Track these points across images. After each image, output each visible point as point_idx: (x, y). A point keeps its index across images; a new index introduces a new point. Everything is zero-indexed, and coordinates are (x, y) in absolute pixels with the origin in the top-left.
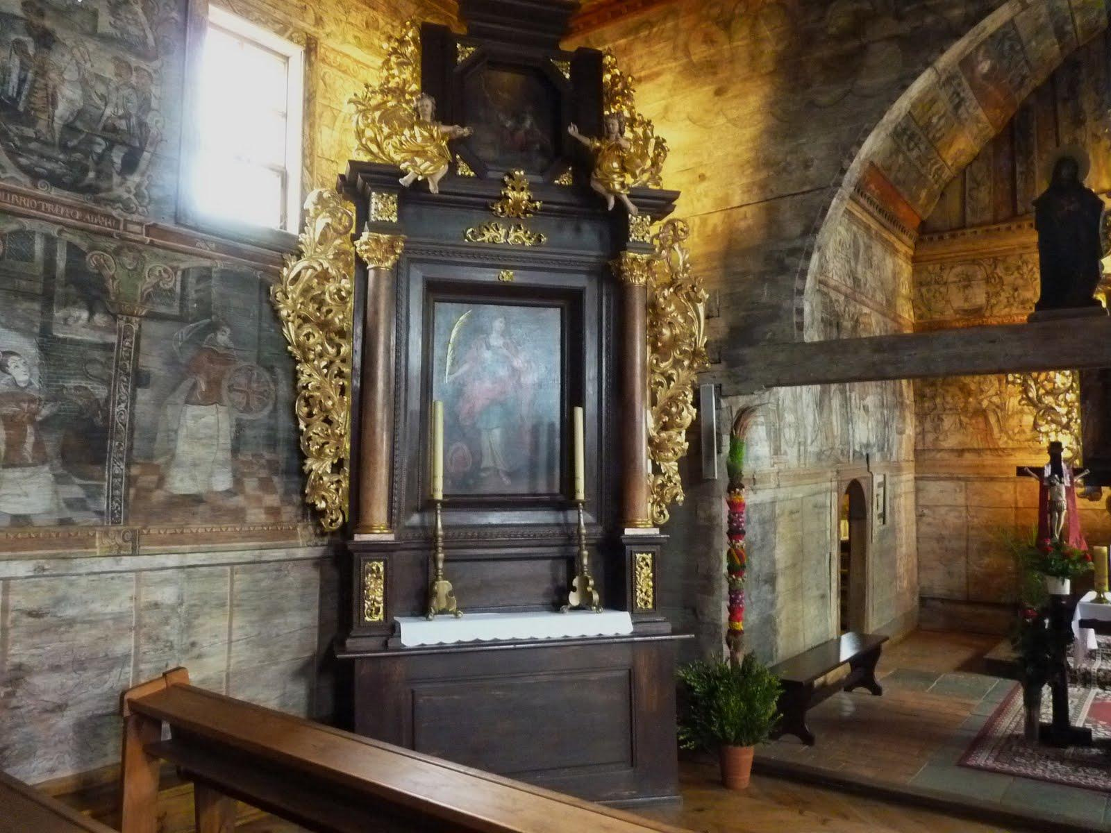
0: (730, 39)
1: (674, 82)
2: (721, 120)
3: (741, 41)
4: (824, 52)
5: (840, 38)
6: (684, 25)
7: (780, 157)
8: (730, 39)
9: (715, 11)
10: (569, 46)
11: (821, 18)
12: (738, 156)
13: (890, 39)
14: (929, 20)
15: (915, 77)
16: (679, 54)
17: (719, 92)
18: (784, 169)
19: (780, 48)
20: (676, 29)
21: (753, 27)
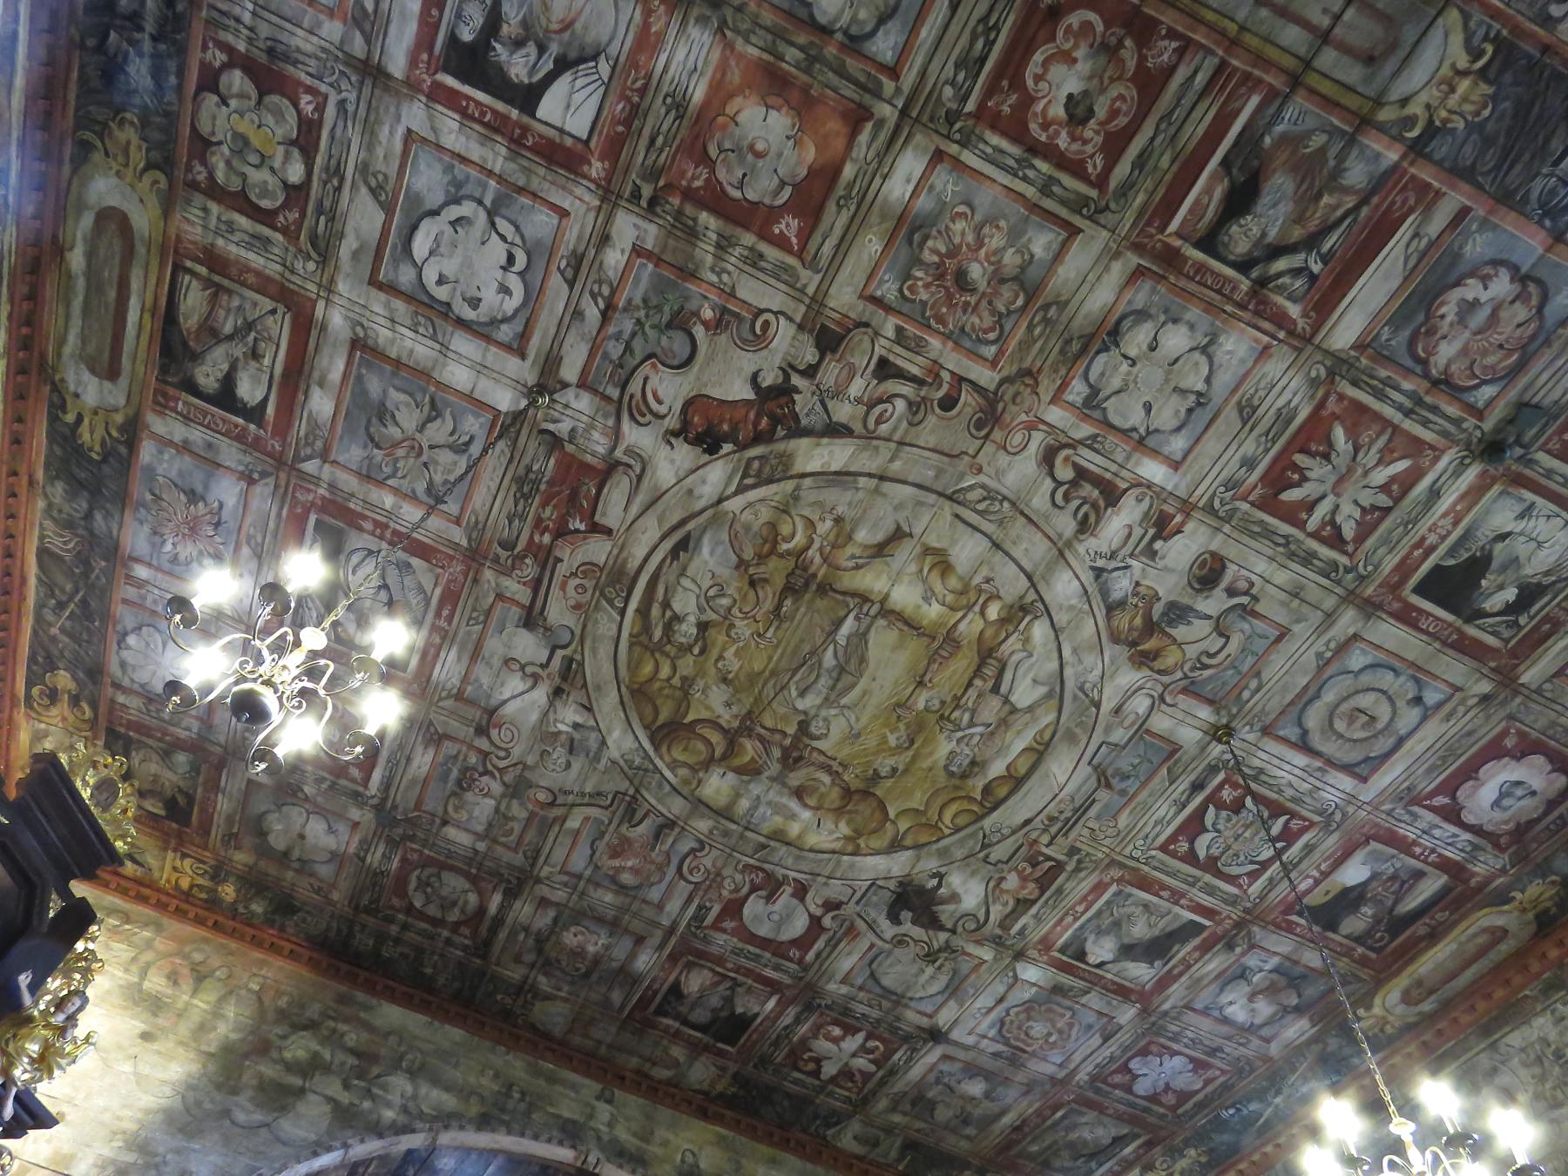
0: (195, 992)
1: (108, 992)
2: (127, 1067)
3: (202, 1004)
4: (269, 1070)
5: (290, 1067)
6: (160, 944)
7: (161, 1150)
8: (195, 992)
9: (198, 957)
10: (79, 889)
11: (284, 1037)
12: (119, 1119)
13: (330, 1100)
14: (367, 1105)
15: (329, 1149)
16: (134, 968)
17: (146, 1036)
18: (156, 1166)
19: (233, 1036)
20: (149, 944)
21: (222, 1000)
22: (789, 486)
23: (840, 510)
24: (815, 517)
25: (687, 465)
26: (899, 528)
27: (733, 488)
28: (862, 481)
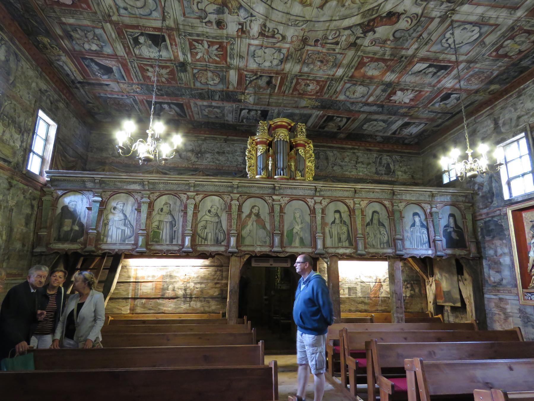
22: (361, 11)
23: (343, 9)
24: (352, 5)
25: (399, 6)
26: (322, 9)
27: (382, 4)
28: (337, 18)
